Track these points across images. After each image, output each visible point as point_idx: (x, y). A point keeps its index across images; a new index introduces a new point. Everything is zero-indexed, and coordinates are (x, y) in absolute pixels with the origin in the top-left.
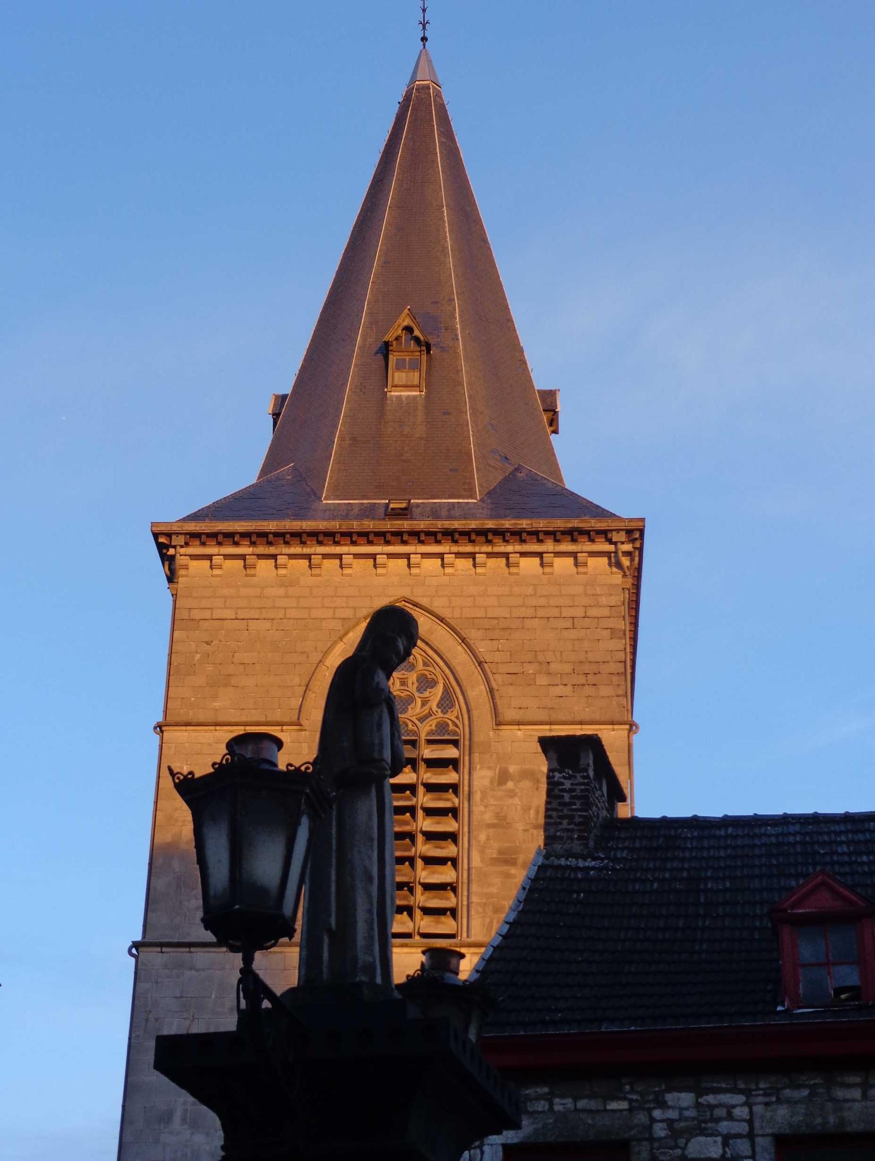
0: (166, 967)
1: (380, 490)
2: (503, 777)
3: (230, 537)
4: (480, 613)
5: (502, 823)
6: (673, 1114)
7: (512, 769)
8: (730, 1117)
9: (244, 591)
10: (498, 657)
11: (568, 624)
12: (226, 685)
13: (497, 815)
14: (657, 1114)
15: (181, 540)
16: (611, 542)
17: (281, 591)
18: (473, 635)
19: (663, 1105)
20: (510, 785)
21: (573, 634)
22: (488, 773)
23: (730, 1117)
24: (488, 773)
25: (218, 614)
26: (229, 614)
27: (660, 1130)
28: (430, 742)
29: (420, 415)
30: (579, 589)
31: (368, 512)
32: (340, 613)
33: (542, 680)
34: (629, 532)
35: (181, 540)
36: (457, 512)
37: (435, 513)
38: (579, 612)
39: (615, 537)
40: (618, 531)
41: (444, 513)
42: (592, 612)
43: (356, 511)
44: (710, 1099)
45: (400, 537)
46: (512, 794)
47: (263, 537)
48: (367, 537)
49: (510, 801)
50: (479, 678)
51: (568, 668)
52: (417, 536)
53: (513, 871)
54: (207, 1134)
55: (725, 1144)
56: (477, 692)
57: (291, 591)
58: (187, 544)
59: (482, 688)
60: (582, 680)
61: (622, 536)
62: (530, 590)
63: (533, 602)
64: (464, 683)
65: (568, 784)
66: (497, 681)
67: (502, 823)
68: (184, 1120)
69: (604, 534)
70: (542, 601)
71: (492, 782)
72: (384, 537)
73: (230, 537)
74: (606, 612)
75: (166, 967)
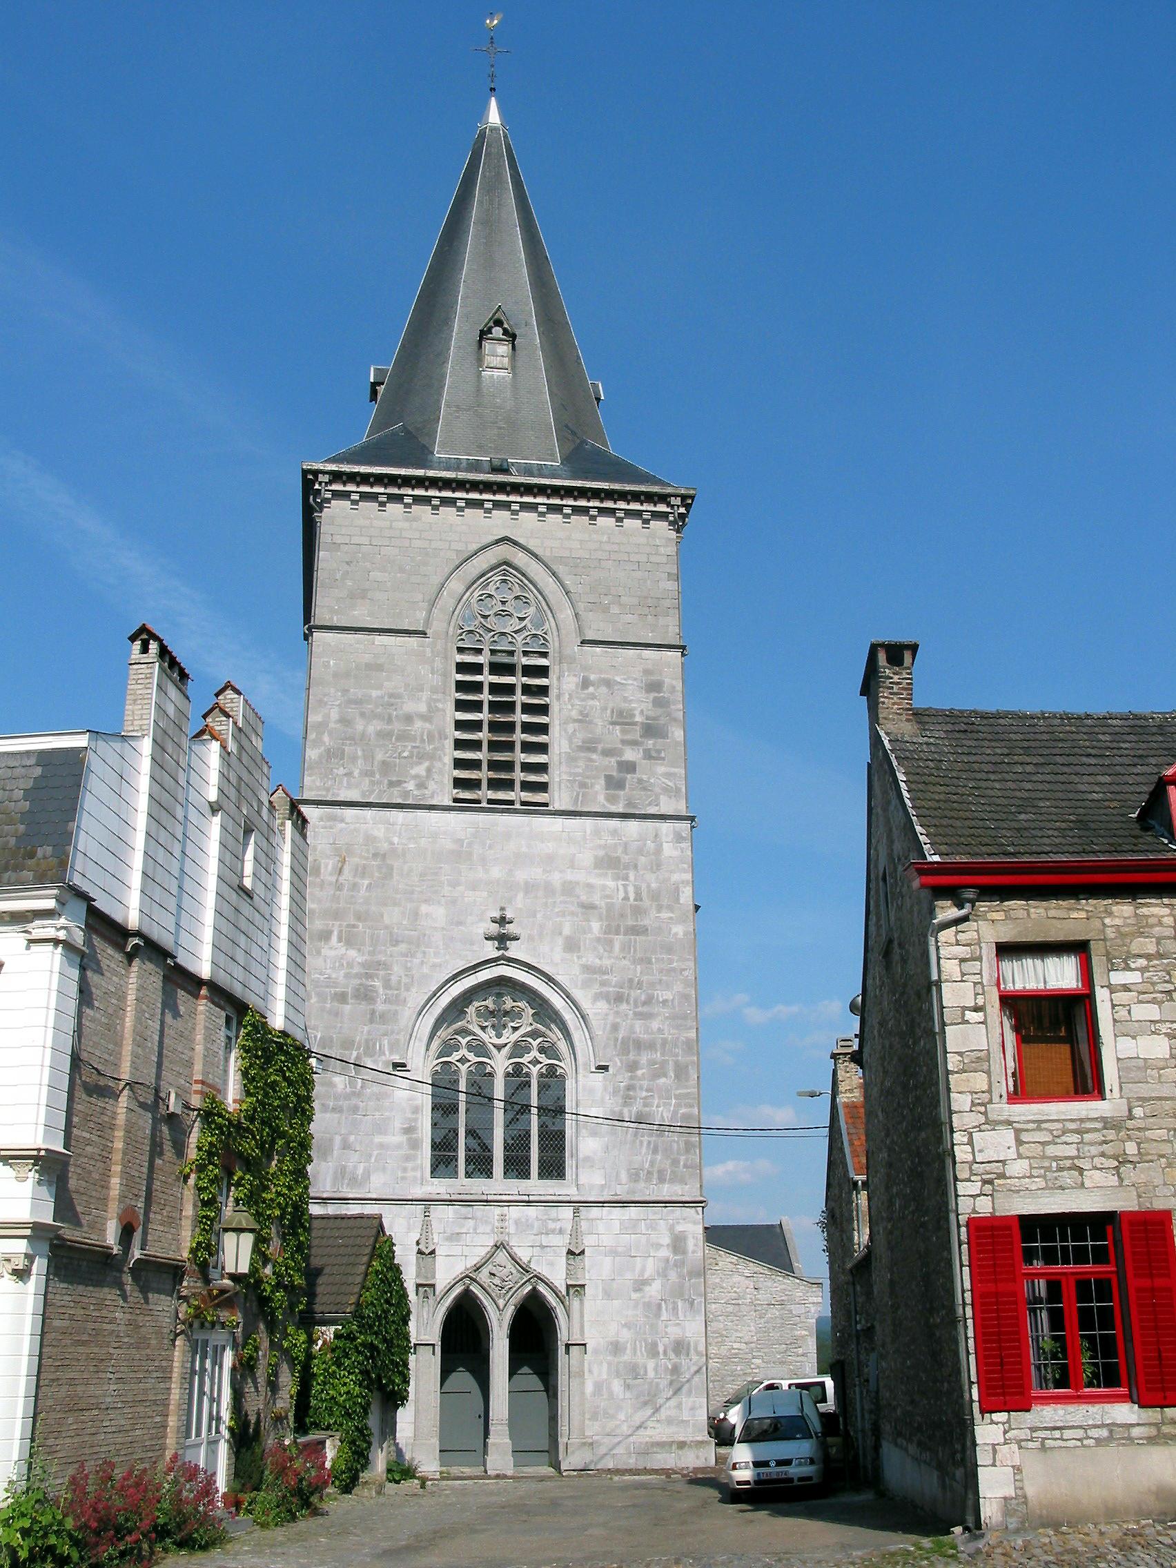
0: (321, 819)
1: (481, 449)
2: (586, 683)
3: (365, 479)
4: (567, 554)
5: (584, 719)
6: (1118, 922)
7: (592, 677)
8: (1160, 924)
9: (376, 523)
10: (580, 589)
11: (636, 567)
12: (363, 598)
13: (581, 713)
14: (1107, 921)
15: (326, 478)
16: (669, 504)
17: (406, 525)
18: (561, 570)
19: (1110, 914)
20: (591, 689)
21: (639, 574)
22: (575, 679)
23: (1160, 924)
24: (575, 679)
25: (355, 540)
26: (365, 540)
27: (1110, 933)
28: (525, 653)
29: (508, 394)
30: (643, 540)
31: (475, 466)
32: (455, 546)
33: (615, 610)
34: (684, 497)
35: (326, 478)
36: (546, 472)
37: (528, 471)
38: (643, 558)
39: (673, 501)
40: (676, 496)
41: (536, 472)
42: (653, 559)
43: (464, 464)
44: (1145, 911)
45: (502, 488)
46: (593, 697)
47: (392, 480)
48: (475, 486)
49: (591, 702)
50: (567, 604)
51: (635, 601)
52: (515, 488)
53: (594, 756)
54: (359, 950)
55: (1158, 943)
56: (565, 614)
57: (415, 524)
58: (330, 482)
59: (569, 612)
60: (646, 611)
61: (678, 501)
62: (605, 538)
63: (607, 547)
64: (554, 608)
65: (896, 678)
66: (581, 606)
67: (584, 719)
68: (340, 940)
69: (663, 498)
70: (616, 548)
71: (577, 685)
72: (487, 487)
73: (365, 479)
74: (664, 560)
75: (321, 819)
